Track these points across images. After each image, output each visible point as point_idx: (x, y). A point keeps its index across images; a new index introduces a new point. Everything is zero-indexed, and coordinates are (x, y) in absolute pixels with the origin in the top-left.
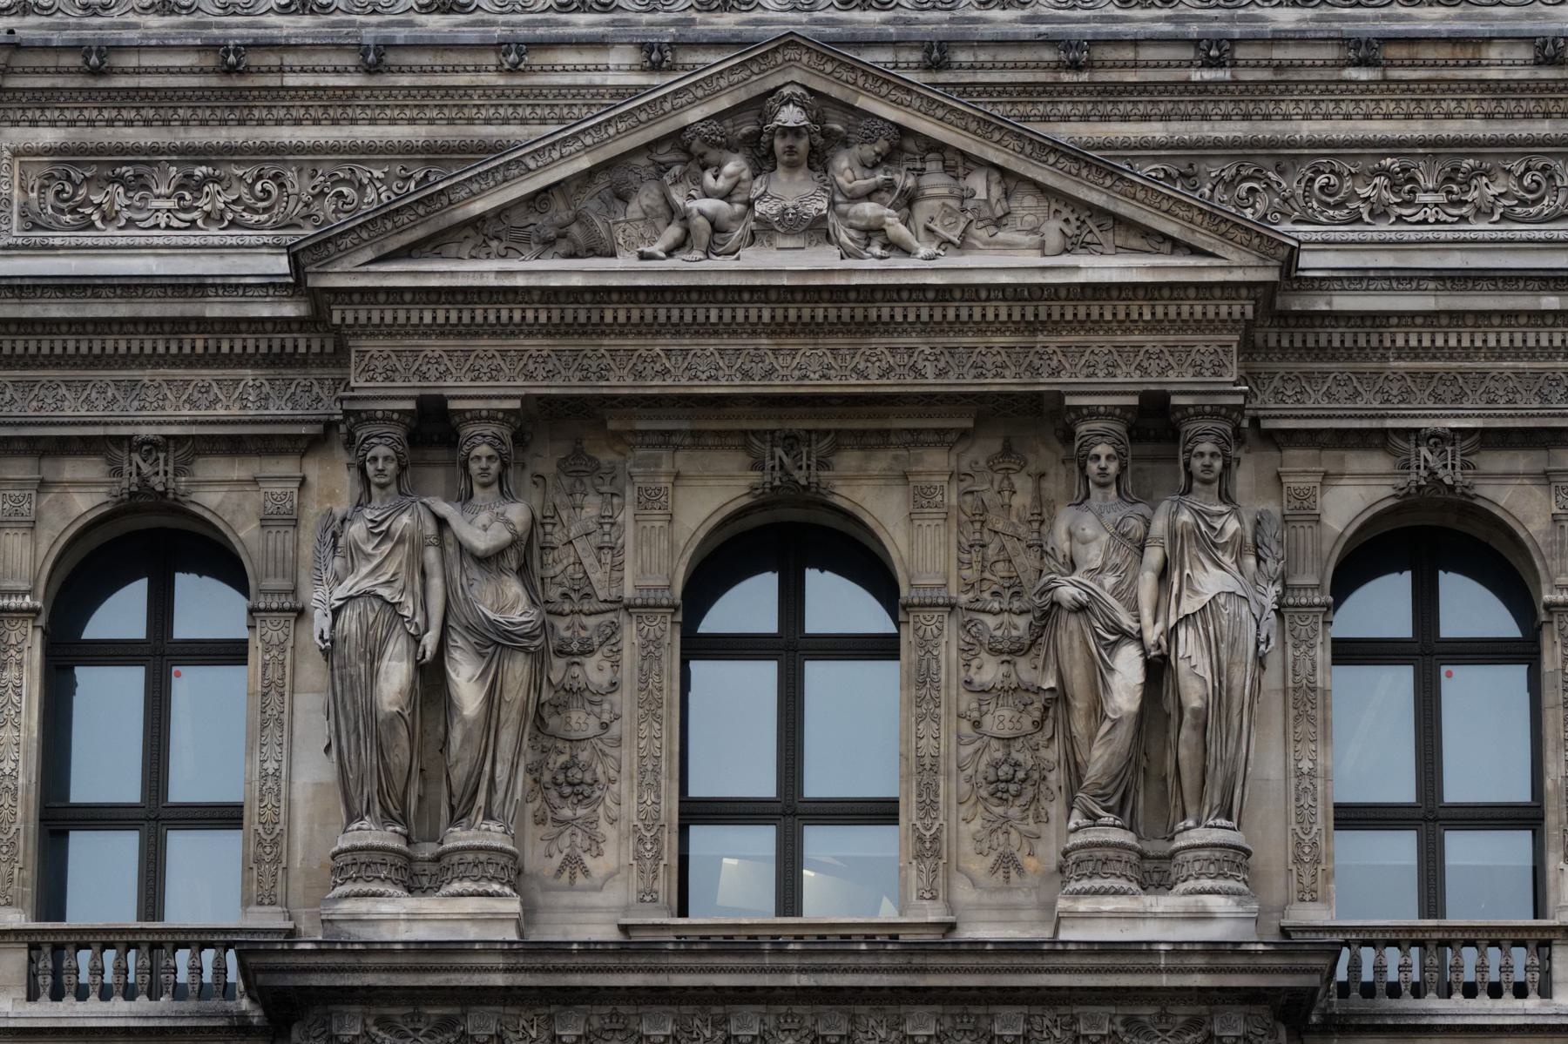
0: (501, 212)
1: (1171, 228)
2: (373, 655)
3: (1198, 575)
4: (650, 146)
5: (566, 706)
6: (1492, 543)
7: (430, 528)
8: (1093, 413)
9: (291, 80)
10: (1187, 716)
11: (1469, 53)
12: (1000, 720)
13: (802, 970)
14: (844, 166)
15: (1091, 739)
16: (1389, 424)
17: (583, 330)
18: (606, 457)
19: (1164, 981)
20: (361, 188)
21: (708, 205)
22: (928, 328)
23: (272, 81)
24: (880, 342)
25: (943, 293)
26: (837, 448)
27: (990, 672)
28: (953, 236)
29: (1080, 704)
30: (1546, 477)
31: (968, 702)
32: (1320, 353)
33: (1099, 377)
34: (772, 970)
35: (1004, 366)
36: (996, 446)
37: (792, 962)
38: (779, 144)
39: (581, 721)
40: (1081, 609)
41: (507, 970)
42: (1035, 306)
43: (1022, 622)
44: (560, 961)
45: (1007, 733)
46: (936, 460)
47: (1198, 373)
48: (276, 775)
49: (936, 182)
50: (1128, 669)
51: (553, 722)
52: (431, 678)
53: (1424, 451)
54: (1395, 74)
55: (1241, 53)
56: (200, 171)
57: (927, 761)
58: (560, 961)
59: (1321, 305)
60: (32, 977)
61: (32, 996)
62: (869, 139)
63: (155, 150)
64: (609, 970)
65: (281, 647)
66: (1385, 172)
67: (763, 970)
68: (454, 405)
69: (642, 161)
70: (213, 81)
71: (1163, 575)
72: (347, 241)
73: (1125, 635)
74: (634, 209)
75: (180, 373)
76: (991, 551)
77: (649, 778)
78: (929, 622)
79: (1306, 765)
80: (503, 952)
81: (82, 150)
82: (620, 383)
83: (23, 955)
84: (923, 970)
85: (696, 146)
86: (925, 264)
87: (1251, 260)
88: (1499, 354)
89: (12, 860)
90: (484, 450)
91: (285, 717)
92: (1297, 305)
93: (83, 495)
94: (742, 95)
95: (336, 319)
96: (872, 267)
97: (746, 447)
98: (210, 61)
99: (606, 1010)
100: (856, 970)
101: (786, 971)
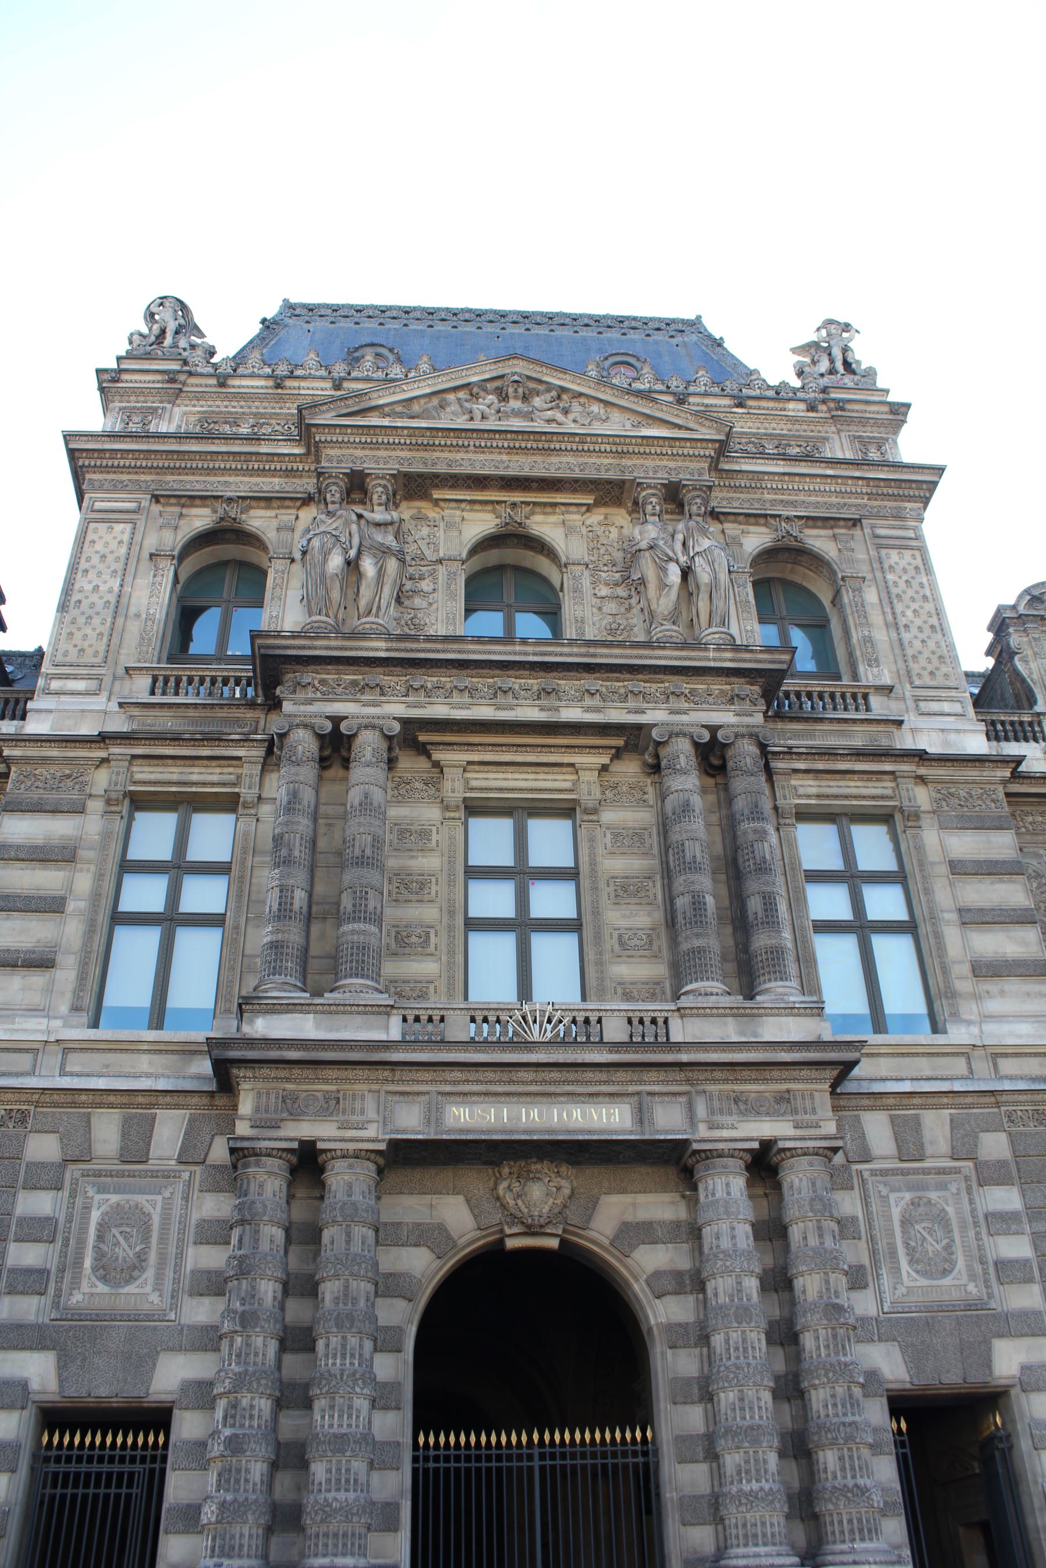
2: (326, 555)
3: (700, 540)
4: (455, 389)
5: (412, 597)
6: (805, 584)
7: (354, 517)
8: (649, 487)
9: (302, 392)
10: (702, 588)
11: (781, 405)
12: (611, 607)
13: (535, 654)
14: (537, 402)
15: (658, 600)
16: (768, 512)
17: (426, 447)
18: (432, 513)
19: (712, 664)
21: (480, 407)
24: (554, 459)
26: (533, 513)
27: (604, 591)
28: (586, 423)
30: (834, 537)
31: (594, 600)
32: (736, 488)
33: (651, 471)
34: (520, 653)
35: (608, 470)
36: (602, 517)
37: (529, 649)
38: (511, 390)
39: (418, 601)
40: (651, 548)
41: (387, 650)
42: (621, 446)
43: (618, 575)
44: (414, 646)
45: (614, 612)
46: (575, 518)
47: (691, 470)
48: (277, 617)
49: (576, 407)
50: (674, 574)
51: (407, 603)
52: (352, 565)
53: (783, 524)
54: (752, 411)
55: (691, 400)
57: (579, 619)
58: (414, 646)
59: (737, 468)
61: (153, 693)
62: (548, 391)
64: (438, 651)
65: (283, 572)
66: (753, 443)
67: (515, 653)
68: (367, 471)
70: (271, 391)
71: (684, 544)
72: (324, 408)
73: (671, 559)
74: (448, 410)
76: (602, 551)
77: (451, 621)
78: (577, 570)
79: (749, 628)
80: (386, 640)
82: (442, 469)
83: (149, 680)
84: (594, 656)
85: (475, 390)
87: (714, 432)
89: (149, 645)
90: (380, 489)
91: (283, 597)
92: (726, 467)
93: (201, 519)
94: (495, 374)
95: (317, 439)
96: (552, 428)
97: (494, 511)
98: (271, 383)
99: (435, 679)
100: (561, 655)
101: (526, 654)
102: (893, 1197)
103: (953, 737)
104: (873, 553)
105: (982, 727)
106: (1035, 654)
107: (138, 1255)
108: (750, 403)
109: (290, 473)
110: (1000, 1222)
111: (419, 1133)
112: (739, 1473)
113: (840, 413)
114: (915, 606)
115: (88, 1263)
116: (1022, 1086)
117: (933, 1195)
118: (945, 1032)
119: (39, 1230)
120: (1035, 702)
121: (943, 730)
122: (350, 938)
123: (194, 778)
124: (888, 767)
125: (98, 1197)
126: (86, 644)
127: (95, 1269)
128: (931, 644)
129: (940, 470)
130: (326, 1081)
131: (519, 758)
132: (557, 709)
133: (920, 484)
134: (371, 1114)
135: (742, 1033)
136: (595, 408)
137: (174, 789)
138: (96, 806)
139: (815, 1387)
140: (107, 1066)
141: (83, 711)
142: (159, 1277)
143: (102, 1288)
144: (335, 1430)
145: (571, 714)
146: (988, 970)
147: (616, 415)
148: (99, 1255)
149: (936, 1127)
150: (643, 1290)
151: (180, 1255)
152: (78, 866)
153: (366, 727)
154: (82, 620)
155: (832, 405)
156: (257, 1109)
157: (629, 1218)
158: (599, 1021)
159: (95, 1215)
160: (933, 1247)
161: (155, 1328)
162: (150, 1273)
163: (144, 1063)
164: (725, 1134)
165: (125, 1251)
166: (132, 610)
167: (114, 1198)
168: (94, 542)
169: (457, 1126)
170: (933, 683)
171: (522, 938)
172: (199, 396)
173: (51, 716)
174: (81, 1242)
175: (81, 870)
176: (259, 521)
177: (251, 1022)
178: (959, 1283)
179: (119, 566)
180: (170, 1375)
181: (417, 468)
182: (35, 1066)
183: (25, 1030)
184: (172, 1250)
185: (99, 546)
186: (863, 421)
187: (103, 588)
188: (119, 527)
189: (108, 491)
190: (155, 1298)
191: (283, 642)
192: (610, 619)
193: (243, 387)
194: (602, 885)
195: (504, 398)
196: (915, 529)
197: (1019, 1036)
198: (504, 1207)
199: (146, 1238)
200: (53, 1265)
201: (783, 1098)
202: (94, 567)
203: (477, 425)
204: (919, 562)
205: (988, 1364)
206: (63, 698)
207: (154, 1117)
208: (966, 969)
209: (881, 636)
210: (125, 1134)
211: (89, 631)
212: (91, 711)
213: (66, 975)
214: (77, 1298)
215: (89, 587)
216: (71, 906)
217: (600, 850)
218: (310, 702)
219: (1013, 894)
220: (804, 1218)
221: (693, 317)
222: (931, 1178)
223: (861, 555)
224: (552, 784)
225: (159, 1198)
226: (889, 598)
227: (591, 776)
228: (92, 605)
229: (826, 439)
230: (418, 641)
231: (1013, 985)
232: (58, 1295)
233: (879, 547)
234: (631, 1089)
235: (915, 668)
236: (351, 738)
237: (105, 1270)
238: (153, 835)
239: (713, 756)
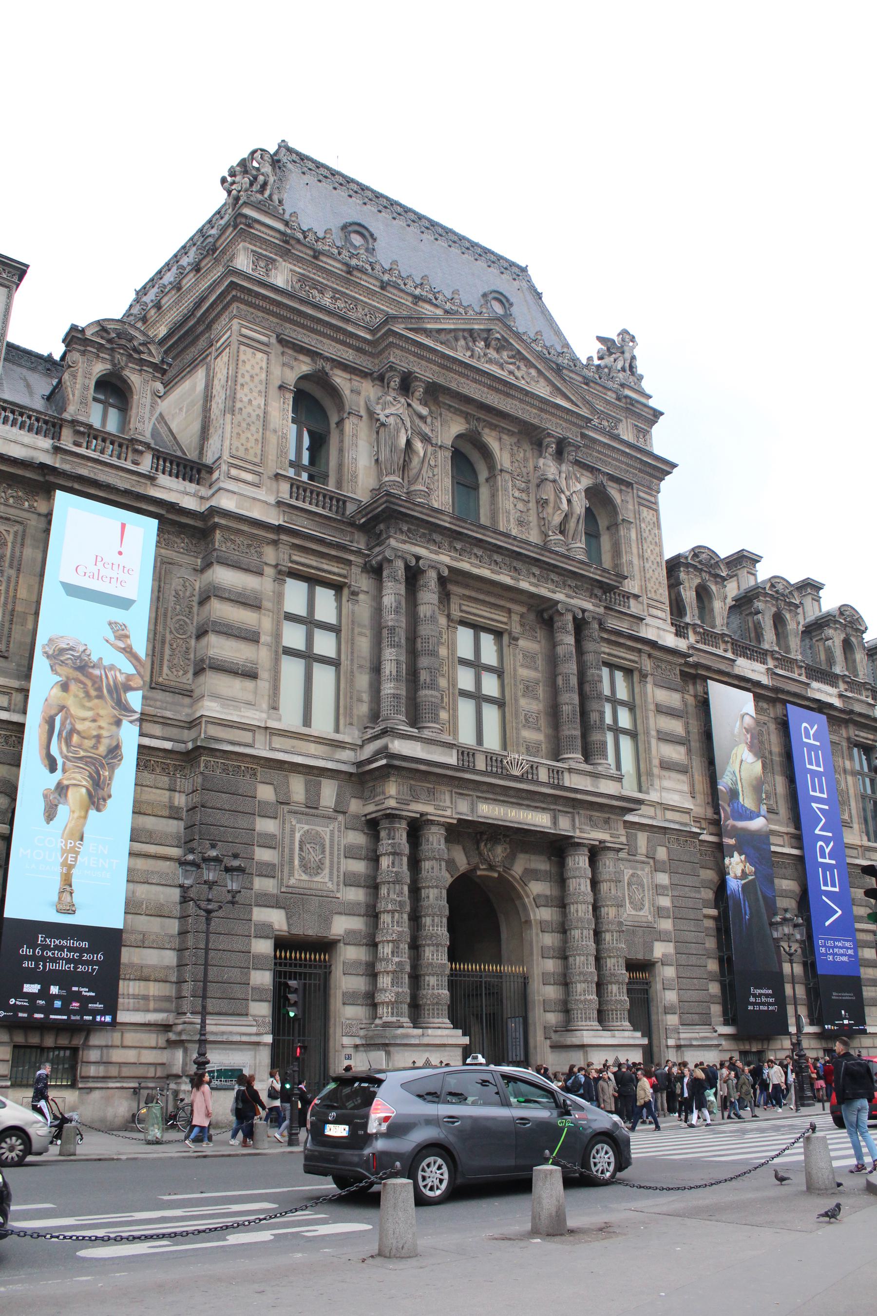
0: (431, 330)
1: (573, 398)
4: (464, 330)
8: (553, 436)
9: (362, 282)
11: (604, 391)
12: (520, 506)
13: (517, 546)
14: (505, 354)
19: (591, 575)
20: (376, 318)
22: (522, 401)
23: (358, 281)
24: (510, 401)
25: (527, 393)
27: (517, 494)
29: (551, 505)
30: (621, 491)
33: (556, 427)
36: (516, 440)
37: (516, 543)
38: (493, 343)
44: (463, 525)
52: (409, 443)
56: (337, 296)
60: (291, 493)
62: (512, 350)
63: (326, 285)
64: (473, 531)
69: (461, 334)
70: (344, 274)
72: (400, 320)
75: (333, 344)
81: (308, 277)
82: (453, 386)
84: (543, 555)
86: (522, 384)
88: (614, 459)
93: (305, 366)
97: (466, 418)
98: (344, 268)
100: (529, 550)
101: (513, 545)
102: (625, 871)
103: (662, 632)
104: (636, 507)
105: (673, 629)
106: (690, 587)
107: (320, 860)
108: (592, 385)
109: (359, 350)
110: (659, 890)
111: (467, 815)
112: (584, 991)
113: (630, 407)
114: (652, 547)
115: (296, 862)
116: (677, 827)
117: (639, 873)
118: (648, 793)
119: (269, 842)
120: (686, 614)
121: (658, 628)
122: (430, 699)
123: (325, 567)
124: (639, 646)
125: (298, 826)
126: (249, 445)
127: (300, 866)
128: (657, 574)
129: (674, 466)
130: (429, 782)
131: (487, 599)
132: (518, 580)
133: (661, 468)
134: (448, 803)
135: (592, 785)
136: (533, 372)
137: (313, 571)
138: (269, 571)
139: (610, 957)
140: (293, 747)
141: (254, 499)
142: (331, 874)
143: (304, 877)
144: (439, 961)
145: (524, 585)
146: (667, 766)
147: (542, 382)
148: (302, 859)
149: (642, 839)
150: (530, 902)
151: (339, 863)
152: (263, 611)
153: (432, 567)
154: (244, 425)
155: (628, 401)
156: (398, 793)
157: (528, 867)
158: (537, 768)
159: (298, 836)
160: (638, 896)
161: (331, 901)
162: (327, 871)
163: (313, 748)
164: (585, 835)
165: (313, 857)
166: (272, 426)
167: (306, 827)
168: (244, 362)
169: (483, 815)
170: (655, 598)
171: (483, 707)
172: (300, 260)
173: (236, 497)
174: (292, 850)
175: (265, 615)
176: (340, 379)
177: (392, 742)
178: (646, 914)
179: (262, 388)
180: (340, 926)
181: (441, 381)
182: (254, 740)
183: (248, 717)
184: (336, 860)
185: (248, 367)
186: (639, 416)
187: (255, 403)
188: (260, 355)
189: (249, 322)
190: (329, 885)
191: (400, 502)
192: (519, 514)
193: (328, 264)
194: (518, 683)
195: (487, 346)
196: (655, 497)
197: (675, 801)
198: (480, 854)
199: (323, 852)
200: (276, 862)
201: (607, 821)
202: (247, 383)
203: (473, 362)
204: (655, 519)
205: (652, 951)
206: (241, 485)
207: (320, 783)
208: (656, 762)
209: (636, 561)
210: (307, 791)
211: (249, 436)
212: (259, 500)
213: (264, 685)
214: (292, 881)
215: (246, 399)
216: (264, 638)
217: (518, 664)
218: (405, 542)
219: (676, 727)
220: (610, 881)
221: (524, 266)
222: (639, 865)
223: (630, 507)
224: (498, 618)
225: (327, 830)
226: (641, 539)
227: (516, 618)
228: (249, 415)
229: (621, 421)
230: (466, 522)
231: (674, 775)
232: (282, 879)
233: (640, 504)
234: (552, 807)
235: (648, 585)
236: (423, 572)
237: (305, 867)
238: (295, 595)
239: (580, 625)
